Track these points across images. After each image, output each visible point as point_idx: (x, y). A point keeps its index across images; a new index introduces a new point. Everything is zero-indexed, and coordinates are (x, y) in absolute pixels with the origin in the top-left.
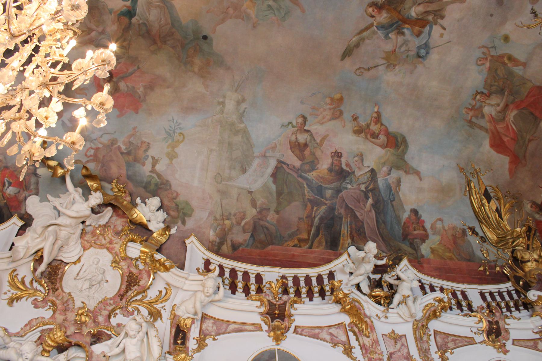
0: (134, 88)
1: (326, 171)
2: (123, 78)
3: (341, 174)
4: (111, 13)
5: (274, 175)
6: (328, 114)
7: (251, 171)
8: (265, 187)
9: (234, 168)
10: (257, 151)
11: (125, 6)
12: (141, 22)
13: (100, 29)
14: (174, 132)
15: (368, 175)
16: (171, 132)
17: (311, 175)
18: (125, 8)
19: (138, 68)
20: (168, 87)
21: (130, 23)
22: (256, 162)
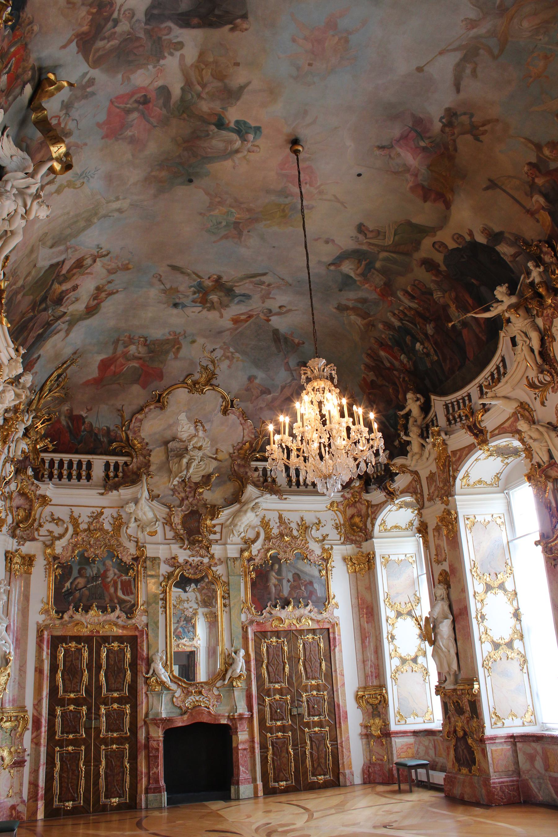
0: (131, 126)
1: (60, 291)
2: (143, 115)
3: (59, 301)
4: (222, 108)
5: (52, 266)
6: (113, 265)
7: (54, 250)
8: (41, 268)
9: (54, 239)
10: (73, 242)
11: (229, 122)
12: (211, 133)
13: (204, 95)
14: (84, 178)
15: (62, 313)
16: (84, 175)
17: (56, 286)
18: (227, 122)
19: (155, 127)
20: (133, 155)
21: (210, 124)
22: (62, 248)
